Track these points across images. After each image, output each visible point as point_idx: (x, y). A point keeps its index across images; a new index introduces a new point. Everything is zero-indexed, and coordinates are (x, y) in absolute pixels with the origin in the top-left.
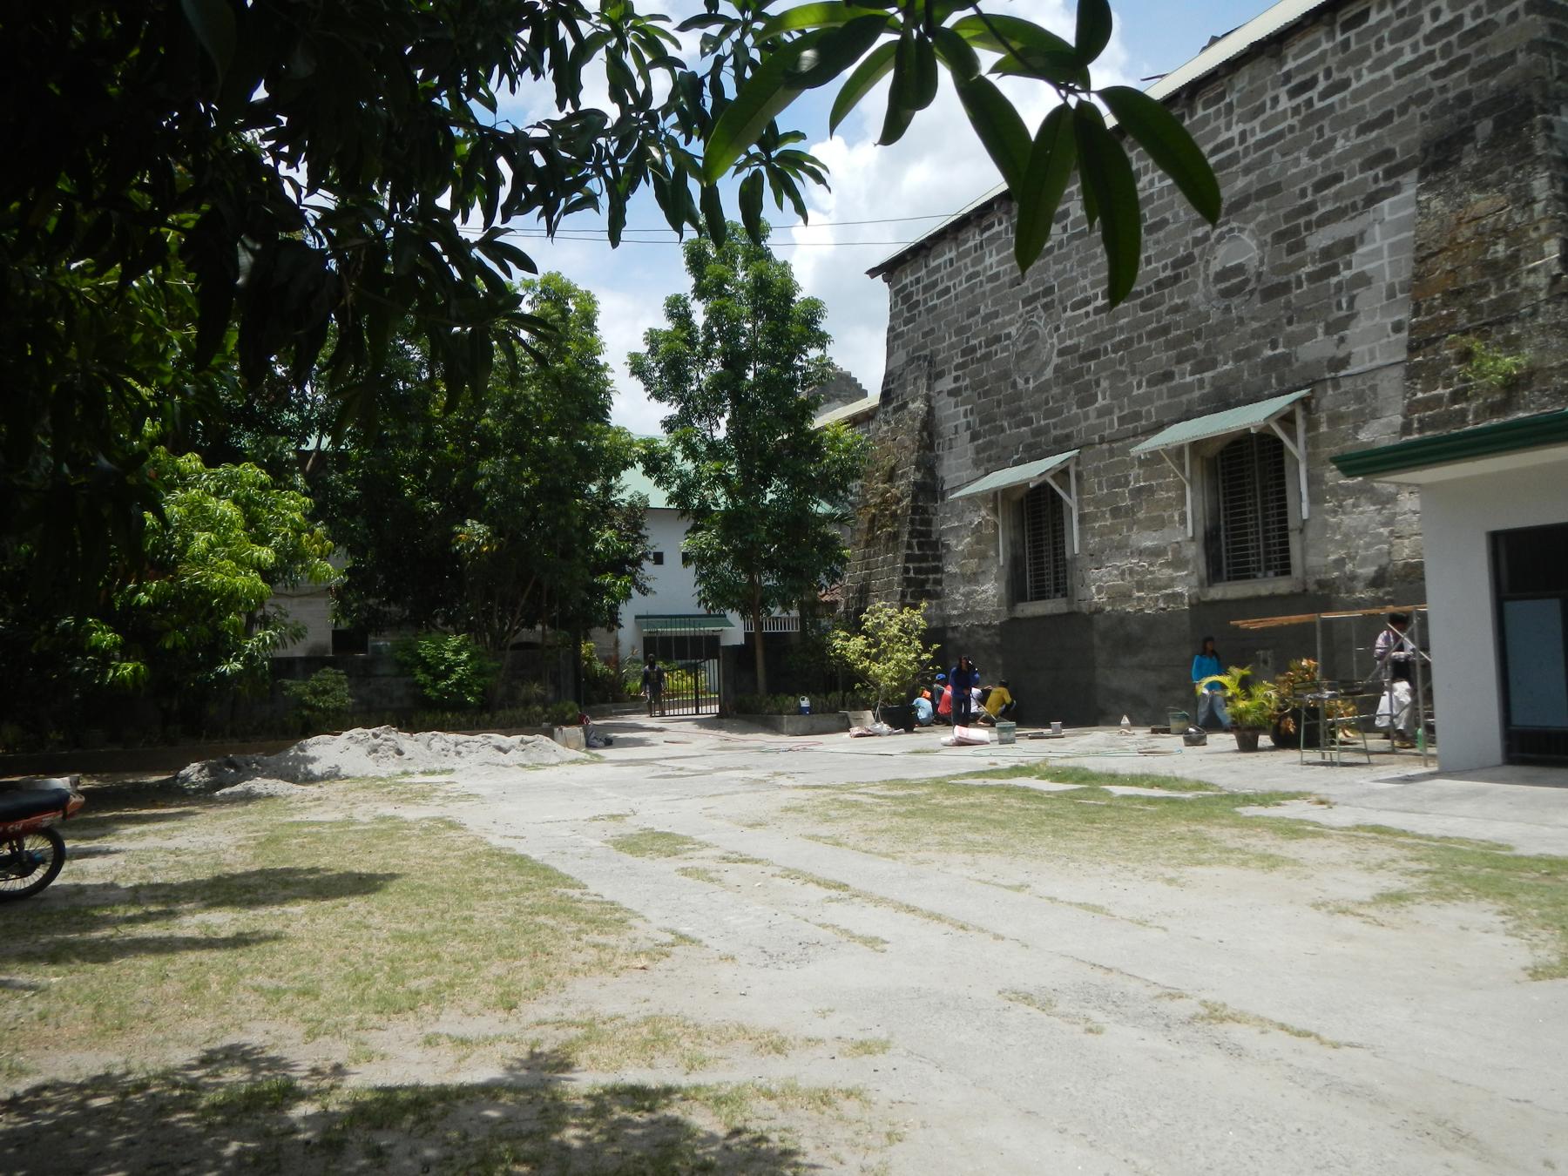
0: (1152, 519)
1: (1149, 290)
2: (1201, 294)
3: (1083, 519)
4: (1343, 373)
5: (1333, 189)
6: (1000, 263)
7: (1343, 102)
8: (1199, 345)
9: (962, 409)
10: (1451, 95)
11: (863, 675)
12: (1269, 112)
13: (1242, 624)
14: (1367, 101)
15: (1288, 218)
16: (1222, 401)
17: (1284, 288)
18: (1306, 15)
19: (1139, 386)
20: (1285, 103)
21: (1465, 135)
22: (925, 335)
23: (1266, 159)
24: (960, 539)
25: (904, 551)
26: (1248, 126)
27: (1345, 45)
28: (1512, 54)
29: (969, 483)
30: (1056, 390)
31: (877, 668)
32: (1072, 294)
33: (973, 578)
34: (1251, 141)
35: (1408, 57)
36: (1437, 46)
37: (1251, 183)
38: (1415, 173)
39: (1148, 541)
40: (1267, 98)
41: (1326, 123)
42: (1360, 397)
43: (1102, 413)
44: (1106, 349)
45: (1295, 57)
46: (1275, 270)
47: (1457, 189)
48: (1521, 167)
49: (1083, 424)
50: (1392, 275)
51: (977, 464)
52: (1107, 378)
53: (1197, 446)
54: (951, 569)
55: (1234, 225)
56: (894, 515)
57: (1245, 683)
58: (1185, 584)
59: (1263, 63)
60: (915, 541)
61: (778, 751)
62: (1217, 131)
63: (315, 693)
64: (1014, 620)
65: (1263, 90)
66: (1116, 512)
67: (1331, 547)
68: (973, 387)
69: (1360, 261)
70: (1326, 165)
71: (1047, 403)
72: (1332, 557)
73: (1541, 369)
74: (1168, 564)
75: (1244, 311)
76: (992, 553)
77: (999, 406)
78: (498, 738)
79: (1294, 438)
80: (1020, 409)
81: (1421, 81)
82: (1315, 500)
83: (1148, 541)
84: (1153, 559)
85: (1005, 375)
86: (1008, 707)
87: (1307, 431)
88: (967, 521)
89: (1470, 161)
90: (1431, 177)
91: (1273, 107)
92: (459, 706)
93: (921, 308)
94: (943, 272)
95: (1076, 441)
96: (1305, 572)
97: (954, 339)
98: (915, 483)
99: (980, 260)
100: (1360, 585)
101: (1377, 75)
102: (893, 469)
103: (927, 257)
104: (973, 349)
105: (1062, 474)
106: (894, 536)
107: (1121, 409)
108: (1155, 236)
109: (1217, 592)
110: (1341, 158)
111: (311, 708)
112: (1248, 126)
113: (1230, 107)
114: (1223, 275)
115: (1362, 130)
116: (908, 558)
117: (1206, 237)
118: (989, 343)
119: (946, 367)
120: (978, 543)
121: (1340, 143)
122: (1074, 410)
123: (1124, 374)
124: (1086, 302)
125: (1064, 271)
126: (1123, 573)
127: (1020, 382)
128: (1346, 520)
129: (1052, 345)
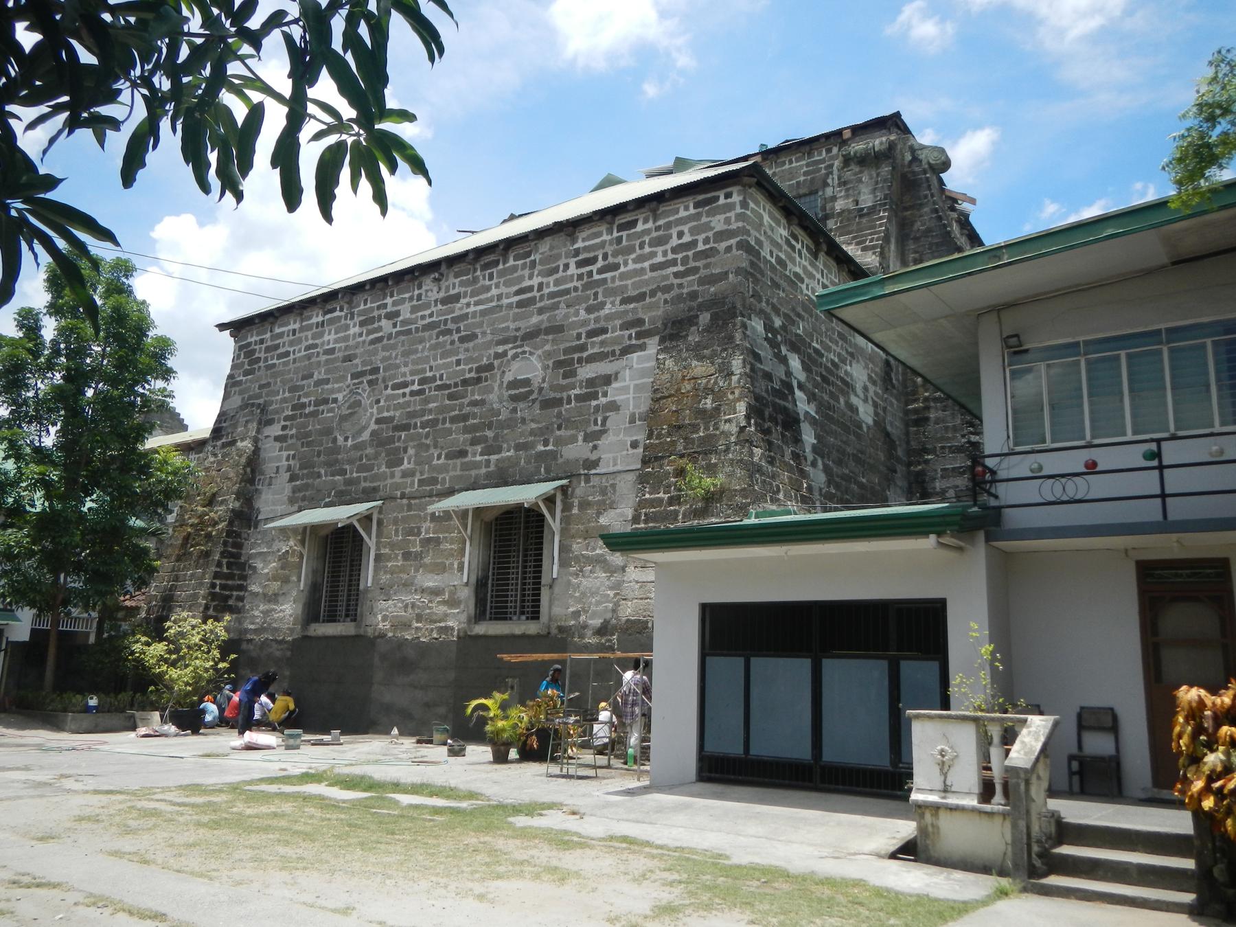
0: (437, 565)
1: (456, 385)
2: (496, 395)
3: (378, 558)
4: (593, 472)
5: (600, 338)
6: (336, 341)
7: (613, 278)
8: (489, 434)
9: (285, 454)
10: (685, 291)
12: (561, 274)
13: (506, 657)
14: (629, 282)
15: (566, 351)
16: (502, 479)
17: (558, 402)
18: (595, 213)
19: (439, 457)
20: (573, 270)
21: (692, 320)
22: (261, 387)
23: (555, 307)
24: (266, 563)
25: (214, 569)
26: (545, 280)
27: (619, 240)
28: (726, 273)
29: (282, 516)
30: (370, 451)
31: (174, 673)
32: (394, 377)
33: (274, 598)
34: (546, 291)
35: (660, 259)
36: (680, 256)
37: (542, 321)
38: (657, 338)
39: (431, 581)
40: (561, 263)
41: (600, 290)
42: (603, 491)
43: (405, 474)
44: (416, 424)
45: (584, 240)
46: (552, 388)
47: (684, 355)
48: (726, 350)
49: (389, 481)
50: (635, 406)
51: (292, 501)
52: (414, 447)
53: (478, 511)
54: (255, 588)
55: (527, 349)
56: (209, 536)
57: (504, 706)
58: (457, 619)
59: (559, 239)
60: (225, 561)
61: (60, 750)
62: (522, 278)
64: (306, 638)
65: (558, 257)
66: (407, 556)
67: (571, 601)
68: (297, 437)
69: (614, 393)
70: (597, 320)
71: (361, 459)
72: (571, 609)
73: (729, 489)
74: (444, 602)
75: (526, 414)
76: (294, 578)
77: (319, 455)
79: (553, 515)
80: (337, 461)
81: (666, 278)
82: (564, 564)
83: (431, 581)
84: (433, 597)
85: (328, 432)
86: (292, 713)
87: (563, 511)
88: (275, 548)
89: (693, 338)
90: (667, 344)
91: (564, 271)
93: (261, 364)
94: (286, 339)
95: (381, 493)
96: (550, 619)
97: (287, 394)
98: (233, 511)
99: (321, 335)
100: (589, 632)
101: (638, 266)
102: (214, 495)
103: (273, 324)
104: (303, 406)
105: (366, 519)
106: (207, 554)
107: (422, 474)
108: (466, 345)
109: (481, 629)
110: (609, 318)
112: (545, 280)
113: (533, 263)
114: (514, 384)
115: (624, 301)
116: (216, 575)
117: (505, 354)
118: (318, 403)
119: (276, 417)
120: (283, 568)
121: (608, 306)
122: (383, 468)
123: (428, 446)
124: (405, 385)
125: (390, 358)
126: (406, 606)
127: (340, 439)
128: (585, 582)
129: (372, 414)
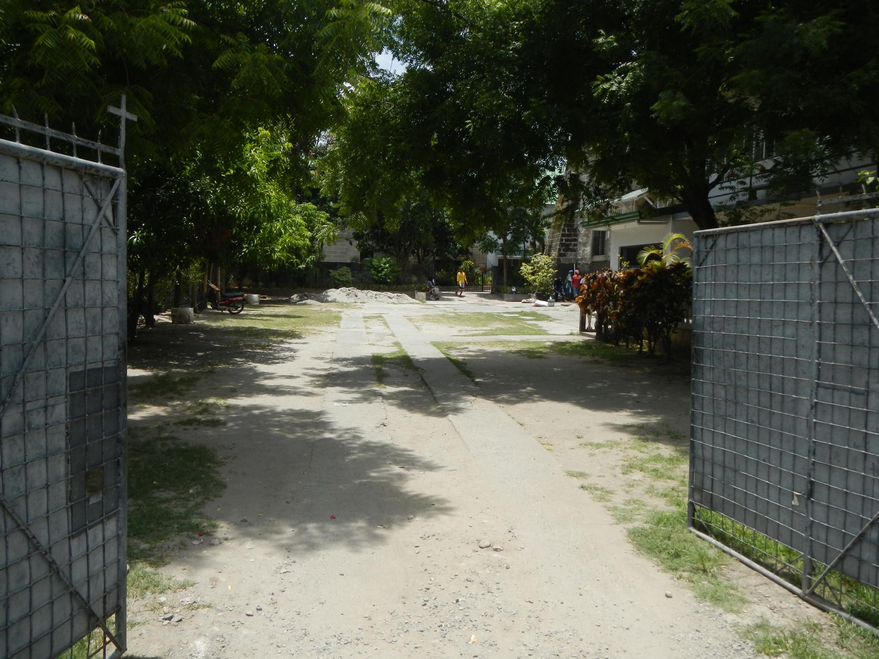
11: (525, 280)
33: (585, 245)
54: (580, 240)
63: (340, 275)
78: (389, 294)
92: (386, 283)
111: (339, 280)
116: (563, 235)
